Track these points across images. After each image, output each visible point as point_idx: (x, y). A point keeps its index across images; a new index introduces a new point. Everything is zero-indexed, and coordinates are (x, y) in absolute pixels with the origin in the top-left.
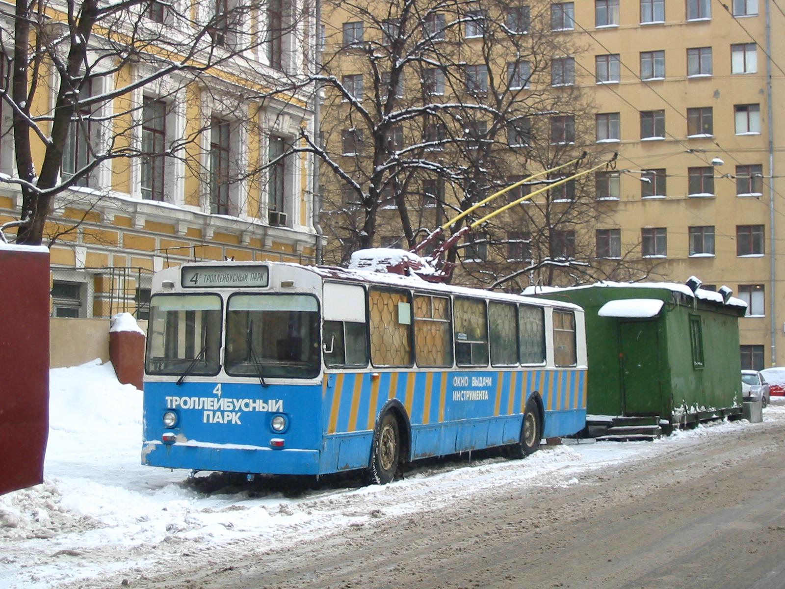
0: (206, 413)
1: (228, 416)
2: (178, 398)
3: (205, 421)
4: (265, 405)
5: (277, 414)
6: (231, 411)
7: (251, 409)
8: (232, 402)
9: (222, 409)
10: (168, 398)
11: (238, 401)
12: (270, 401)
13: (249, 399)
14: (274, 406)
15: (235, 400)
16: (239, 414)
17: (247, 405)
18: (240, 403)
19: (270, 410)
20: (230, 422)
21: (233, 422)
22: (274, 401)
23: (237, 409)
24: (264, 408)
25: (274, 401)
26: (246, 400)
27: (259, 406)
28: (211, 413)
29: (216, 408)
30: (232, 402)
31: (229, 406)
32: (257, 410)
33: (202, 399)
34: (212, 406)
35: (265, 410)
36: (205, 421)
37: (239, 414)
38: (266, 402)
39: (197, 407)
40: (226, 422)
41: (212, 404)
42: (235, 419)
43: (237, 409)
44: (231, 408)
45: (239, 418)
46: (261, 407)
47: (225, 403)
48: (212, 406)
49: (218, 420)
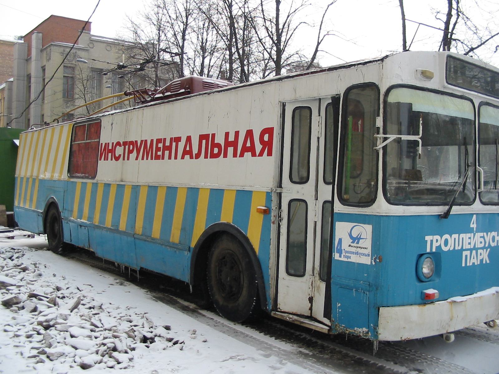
0: (464, 253)
2: (438, 237)
3: (463, 265)
6: (482, 248)
8: (483, 237)
10: (428, 238)
15: (485, 234)
16: (489, 250)
20: (482, 261)
23: (487, 245)
28: (468, 253)
30: (483, 237)
31: (481, 243)
33: (462, 235)
34: (470, 244)
36: (463, 265)
37: (489, 250)
39: (456, 248)
41: (469, 241)
43: (487, 245)
44: (482, 245)
47: (478, 239)
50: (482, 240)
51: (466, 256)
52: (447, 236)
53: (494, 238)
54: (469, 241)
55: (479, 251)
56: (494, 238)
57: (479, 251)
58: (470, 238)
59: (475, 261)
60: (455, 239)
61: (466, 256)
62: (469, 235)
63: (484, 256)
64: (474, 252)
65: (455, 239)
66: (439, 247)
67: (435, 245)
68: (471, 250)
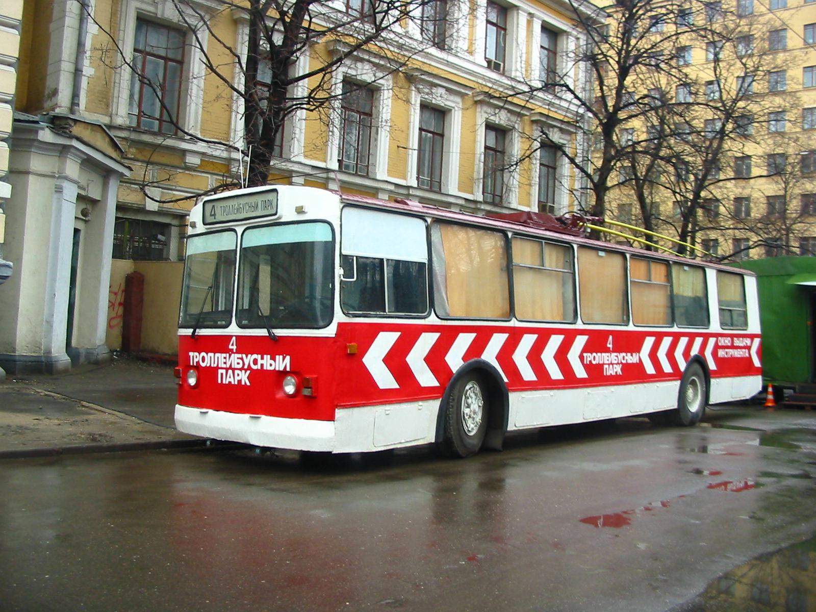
0: (220, 371)
1: (238, 375)
2: (196, 354)
3: (219, 381)
4: (272, 362)
5: (283, 374)
6: (241, 369)
7: (259, 368)
8: (242, 359)
9: (233, 367)
11: (247, 357)
12: (277, 357)
13: (257, 354)
14: (282, 363)
15: (244, 356)
16: (248, 372)
17: (255, 362)
18: (249, 359)
19: (277, 369)
20: (240, 381)
21: (243, 383)
22: (281, 357)
24: (271, 365)
25: (281, 357)
26: (255, 356)
27: (267, 363)
28: (224, 371)
29: (228, 366)
30: (242, 359)
31: (238, 363)
32: (265, 368)
33: (218, 355)
35: (272, 368)
37: (248, 372)
39: (212, 366)
40: (236, 383)
41: (225, 360)
42: (244, 377)
43: (246, 367)
44: (240, 366)
45: (248, 378)
46: (269, 365)
47: (235, 360)
48: (225, 363)
49: (230, 380)
50: (240, 361)
51: (222, 374)
52: (203, 354)
54: (225, 360)
55: (237, 372)
57: (237, 372)
58: (225, 358)
59: (232, 380)
60: (211, 357)
61: (222, 374)
62: (224, 355)
63: (244, 377)
64: (230, 372)
65: (211, 357)
66: (198, 362)
68: (227, 369)
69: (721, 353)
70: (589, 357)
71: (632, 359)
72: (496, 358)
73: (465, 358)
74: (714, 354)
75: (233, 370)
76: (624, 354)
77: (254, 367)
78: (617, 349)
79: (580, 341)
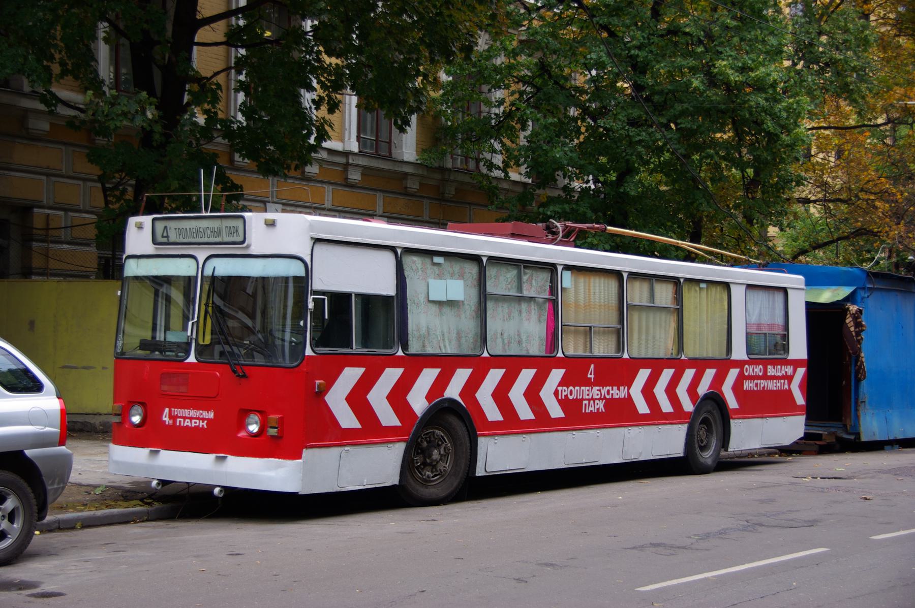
0: (585, 402)
6: (599, 399)
18: (604, 390)
26: (608, 388)
28: (587, 402)
30: (599, 390)
38: (619, 389)
44: (598, 397)
47: (595, 391)
53: (608, 391)
55: (597, 401)
56: (608, 391)
63: (601, 405)
66: (566, 396)
67: (564, 394)
68: (589, 400)
69: (748, 385)
70: (565, 391)
71: (618, 393)
72: (388, 398)
73: (429, 397)
74: (737, 388)
75: (594, 400)
76: (609, 388)
77: (608, 397)
78: (600, 381)
79: (557, 375)
